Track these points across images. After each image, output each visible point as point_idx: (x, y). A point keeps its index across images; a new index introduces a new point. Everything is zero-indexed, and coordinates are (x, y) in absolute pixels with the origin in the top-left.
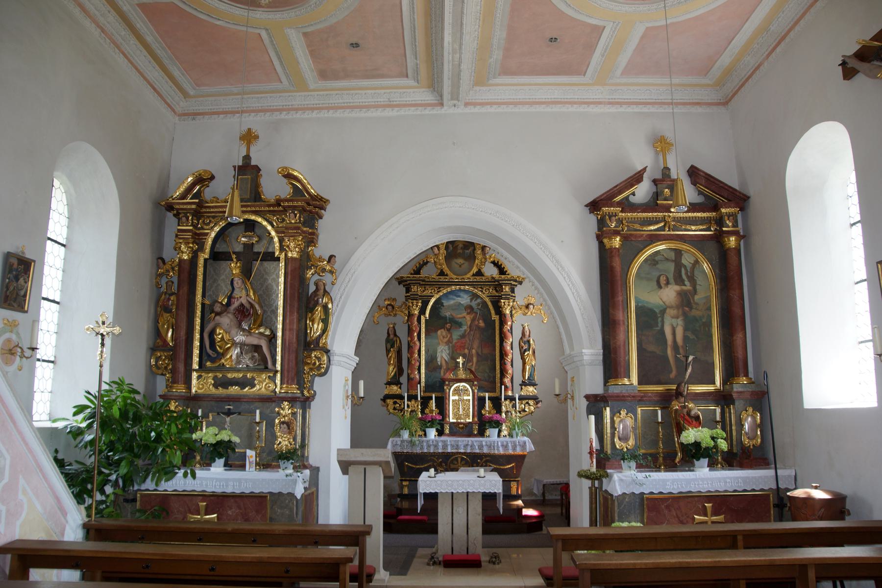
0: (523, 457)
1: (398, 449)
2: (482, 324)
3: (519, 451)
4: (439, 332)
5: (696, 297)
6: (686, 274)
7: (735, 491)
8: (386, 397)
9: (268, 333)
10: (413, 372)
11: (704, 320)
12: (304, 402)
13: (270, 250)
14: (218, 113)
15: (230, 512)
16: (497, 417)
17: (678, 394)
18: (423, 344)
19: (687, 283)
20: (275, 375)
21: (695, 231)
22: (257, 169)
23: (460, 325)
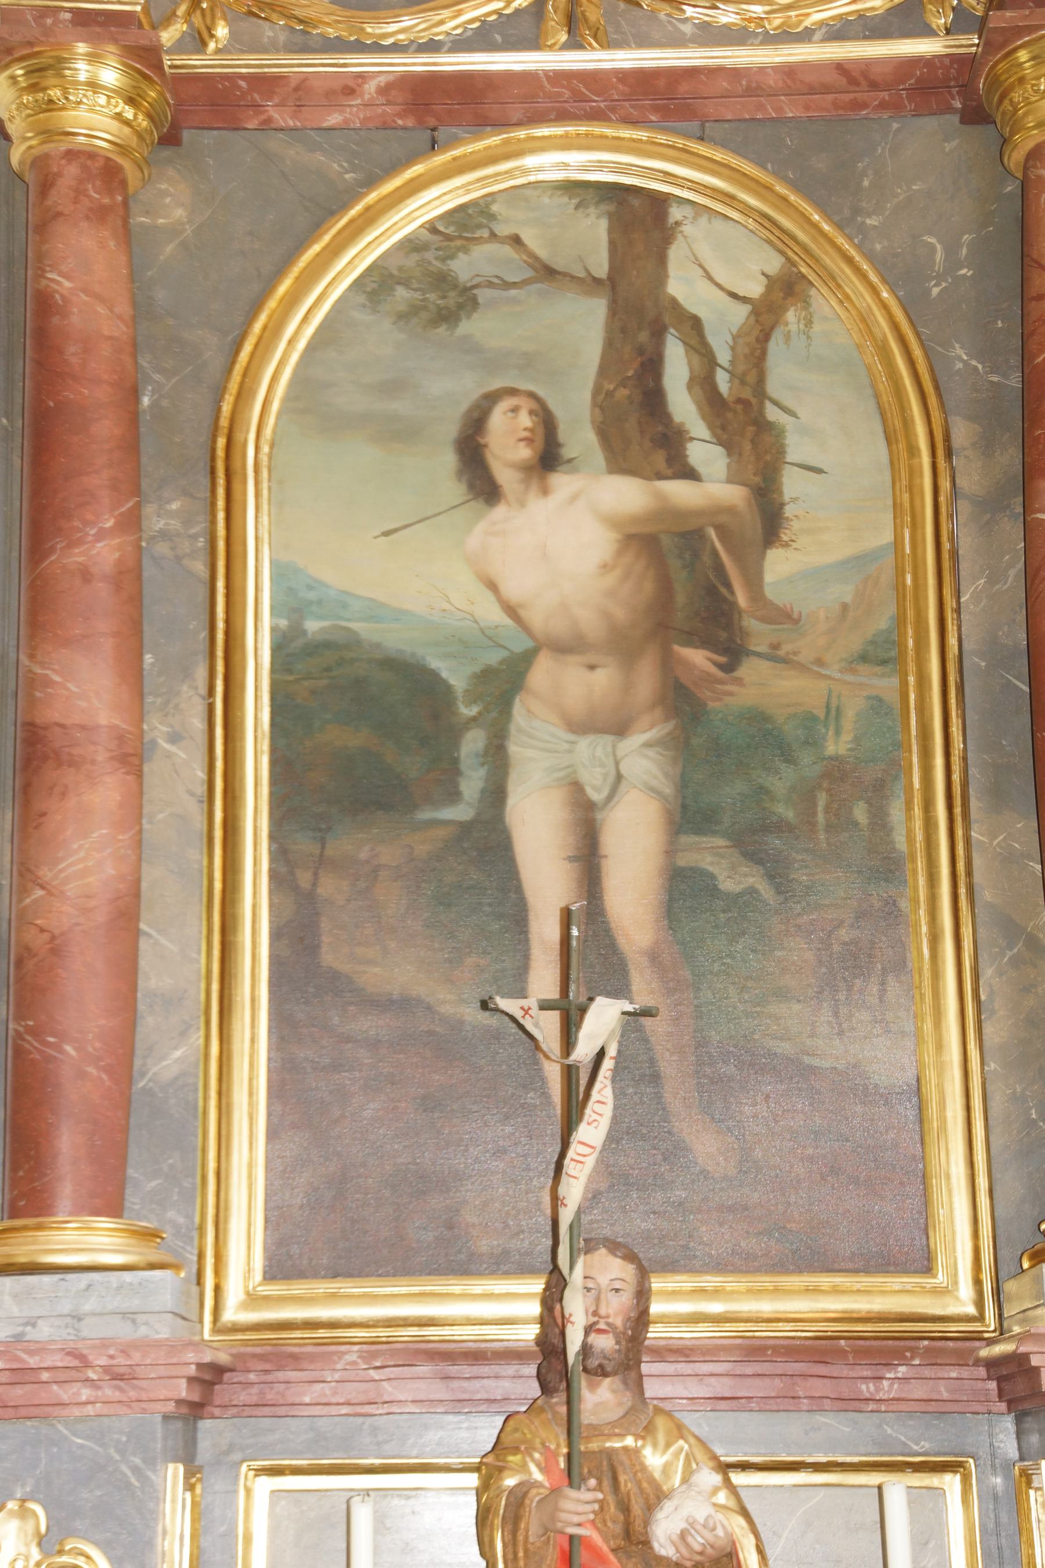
5: (778, 567)
6: (703, 383)
11: (837, 746)
19: (704, 452)
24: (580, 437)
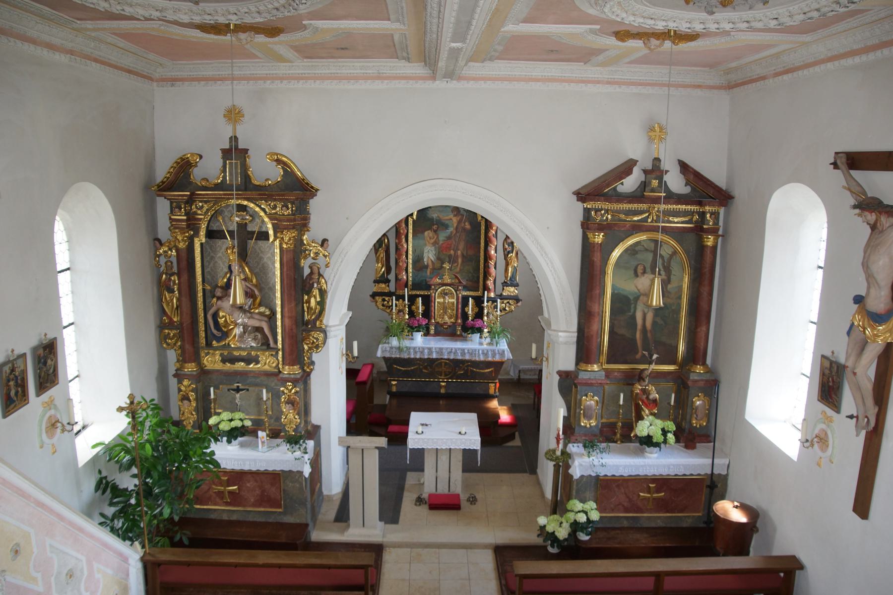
0: (501, 363)
1: (387, 355)
2: (468, 226)
3: (497, 358)
4: (426, 233)
6: (663, 264)
7: (676, 475)
8: (374, 295)
9: (268, 313)
10: (400, 273)
12: (305, 378)
13: (264, 229)
14: (199, 80)
15: (248, 485)
16: (478, 323)
17: (639, 377)
18: (410, 245)
20: (277, 353)
21: (677, 222)
22: (246, 151)
23: (446, 227)
24: (648, 270)
